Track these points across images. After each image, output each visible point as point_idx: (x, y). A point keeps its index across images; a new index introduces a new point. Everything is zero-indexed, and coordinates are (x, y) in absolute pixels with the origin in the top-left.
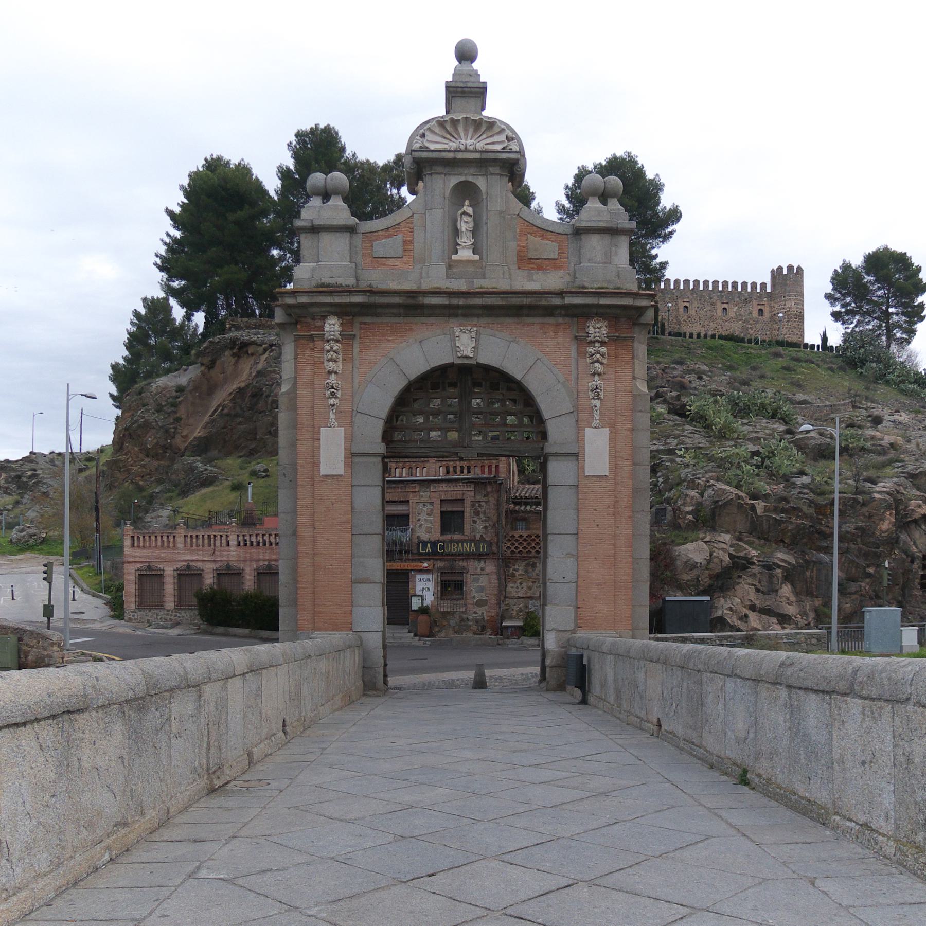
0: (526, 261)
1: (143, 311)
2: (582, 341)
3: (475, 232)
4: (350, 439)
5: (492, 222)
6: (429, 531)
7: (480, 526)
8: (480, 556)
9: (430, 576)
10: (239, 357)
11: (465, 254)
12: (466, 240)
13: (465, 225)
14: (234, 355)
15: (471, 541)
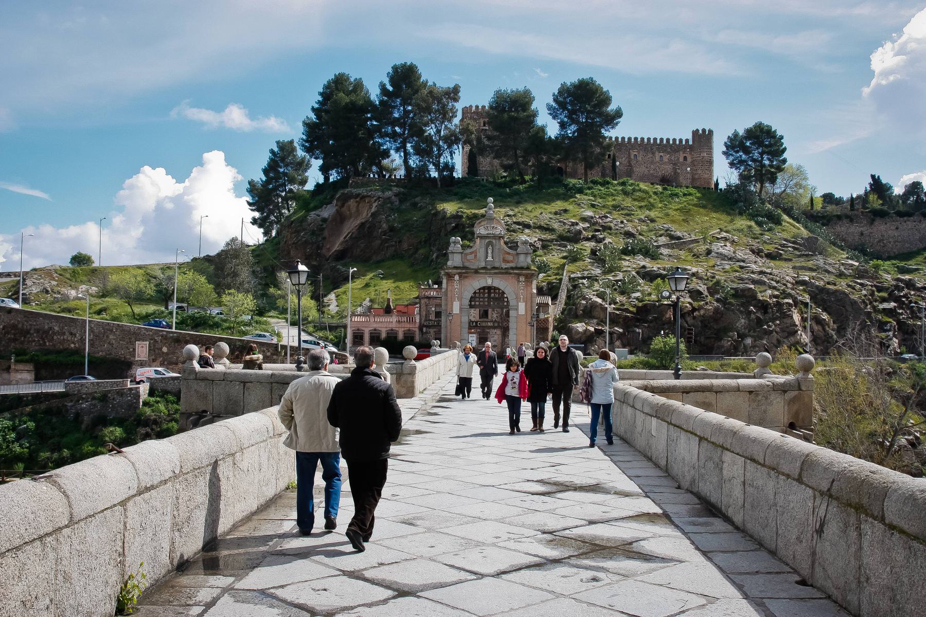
0: (505, 261)
1: (276, 149)
2: (519, 281)
3: (492, 253)
4: (461, 305)
5: (496, 251)
6: (474, 317)
7: (495, 316)
8: (494, 327)
9: (474, 335)
10: (359, 203)
11: (490, 258)
12: (490, 255)
13: (490, 251)
14: (357, 202)
15: (491, 322)
